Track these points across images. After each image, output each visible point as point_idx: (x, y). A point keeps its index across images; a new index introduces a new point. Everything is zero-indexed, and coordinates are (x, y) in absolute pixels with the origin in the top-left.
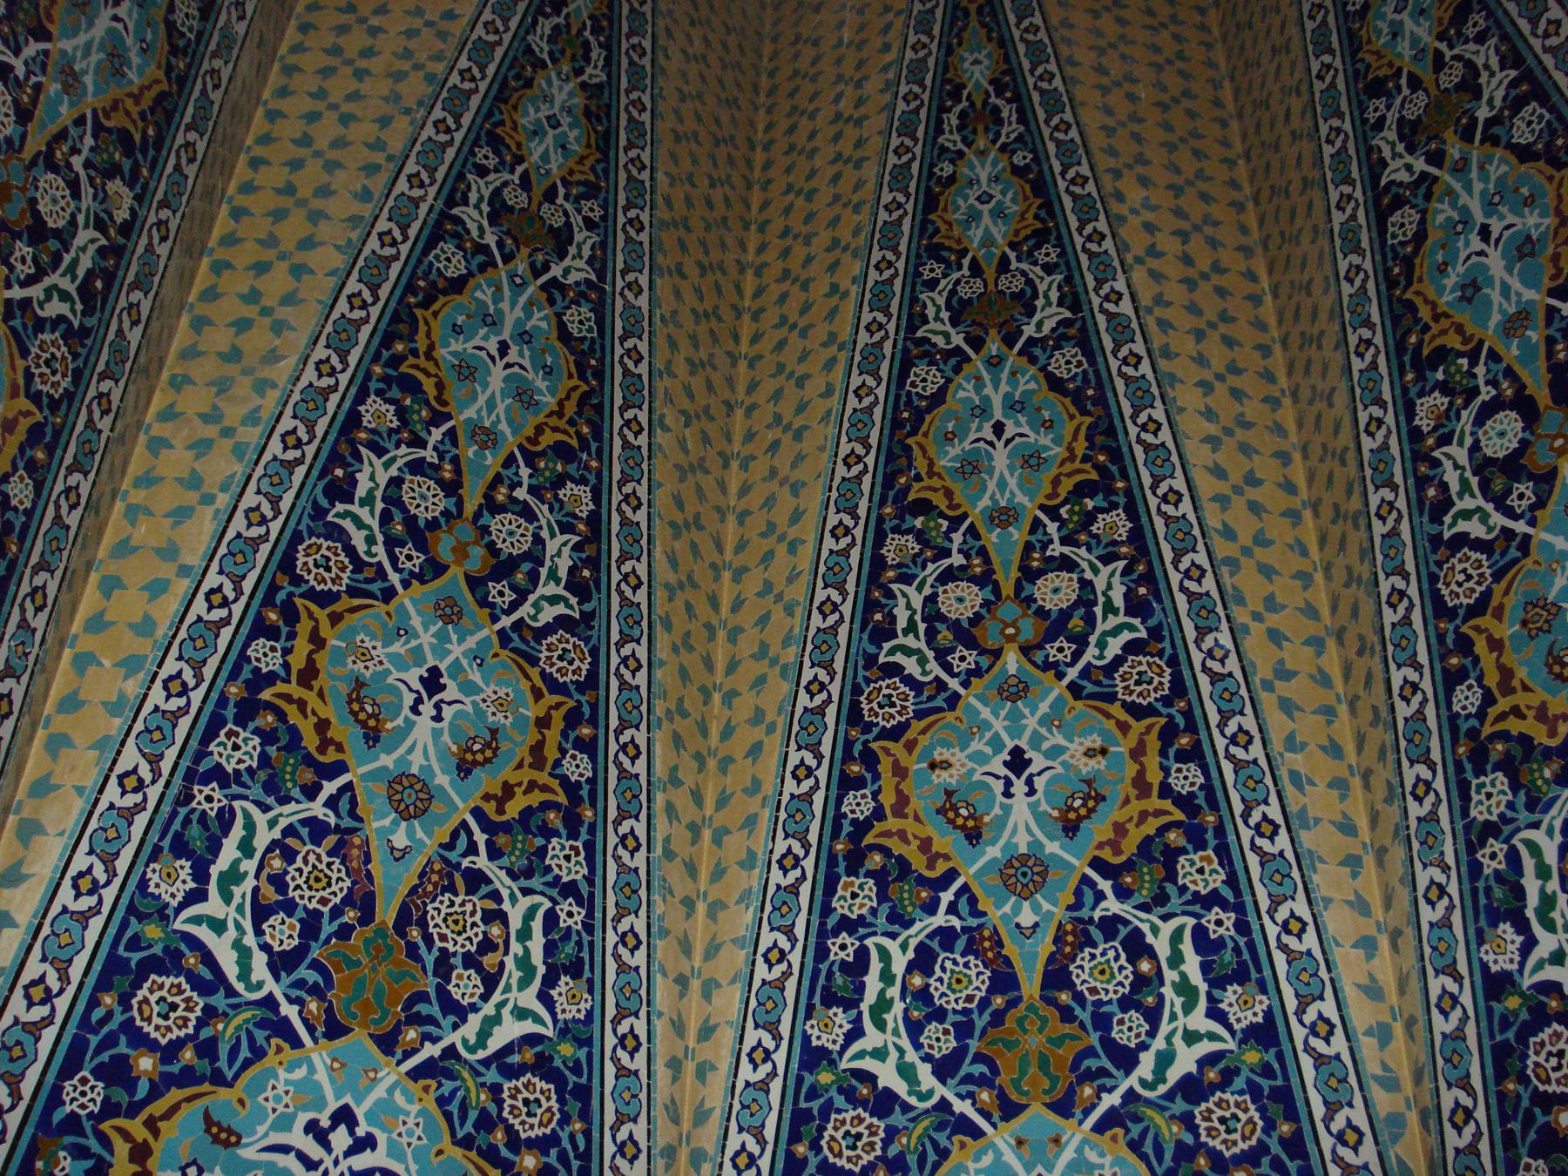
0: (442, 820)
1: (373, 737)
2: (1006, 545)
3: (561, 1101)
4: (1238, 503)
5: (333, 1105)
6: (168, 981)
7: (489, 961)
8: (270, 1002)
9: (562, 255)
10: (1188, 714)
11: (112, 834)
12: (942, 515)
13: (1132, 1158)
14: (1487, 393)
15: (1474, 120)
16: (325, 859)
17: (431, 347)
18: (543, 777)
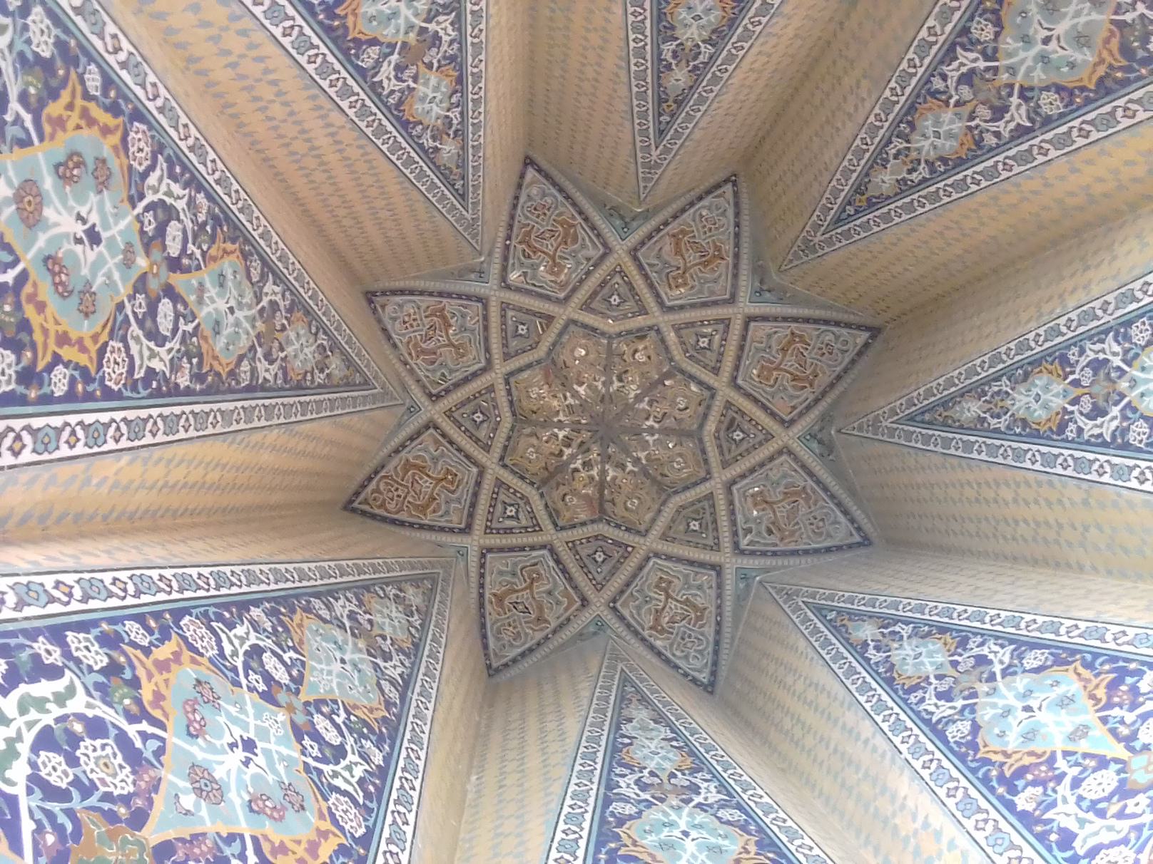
9: (991, 662)
17: (1005, 754)
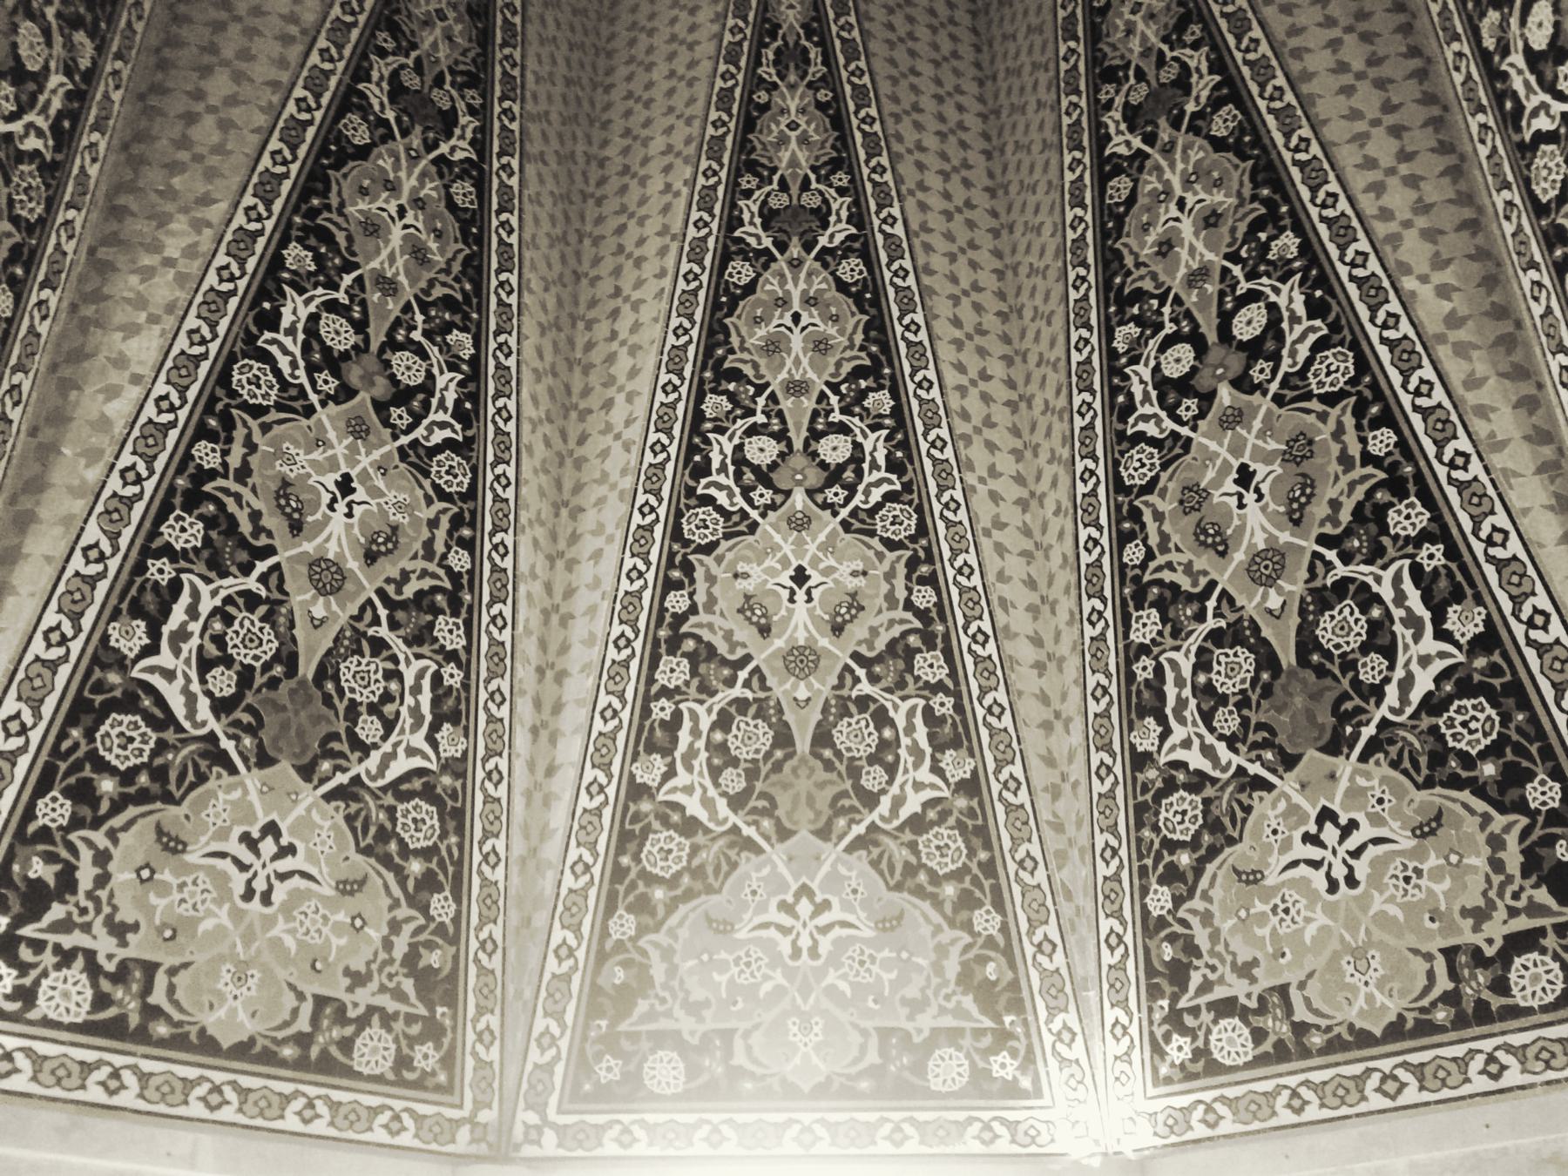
0: (353, 597)
1: (296, 527)
2: (798, 411)
3: (441, 820)
4: (974, 393)
5: (263, 820)
6: (127, 719)
7: (389, 709)
8: (212, 738)
9: (449, 135)
10: (928, 550)
11: (77, 596)
12: (750, 383)
13: (873, 873)
14: (1169, 328)
15: (1183, 112)
16: (258, 624)
17: (342, 205)
18: (432, 567)
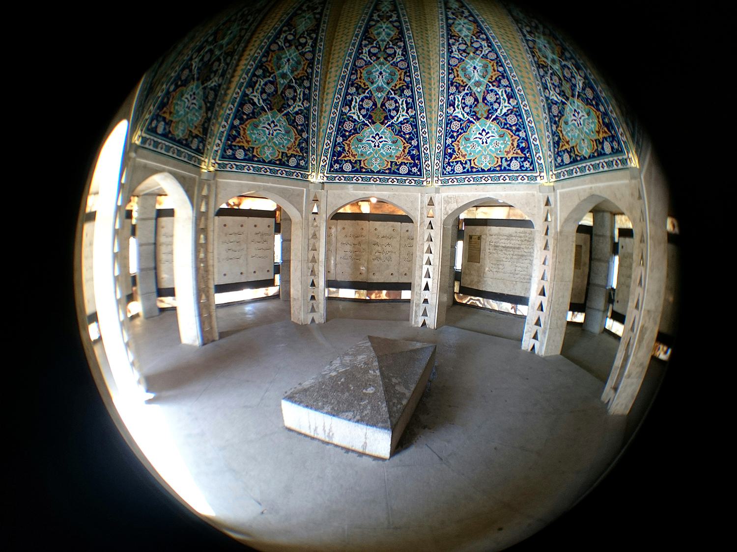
5: (482, 129)
7: (498, 101)
